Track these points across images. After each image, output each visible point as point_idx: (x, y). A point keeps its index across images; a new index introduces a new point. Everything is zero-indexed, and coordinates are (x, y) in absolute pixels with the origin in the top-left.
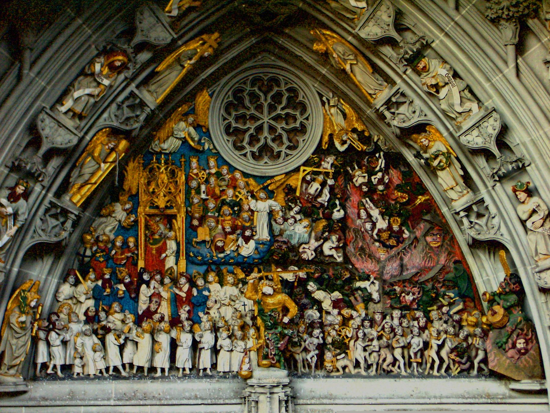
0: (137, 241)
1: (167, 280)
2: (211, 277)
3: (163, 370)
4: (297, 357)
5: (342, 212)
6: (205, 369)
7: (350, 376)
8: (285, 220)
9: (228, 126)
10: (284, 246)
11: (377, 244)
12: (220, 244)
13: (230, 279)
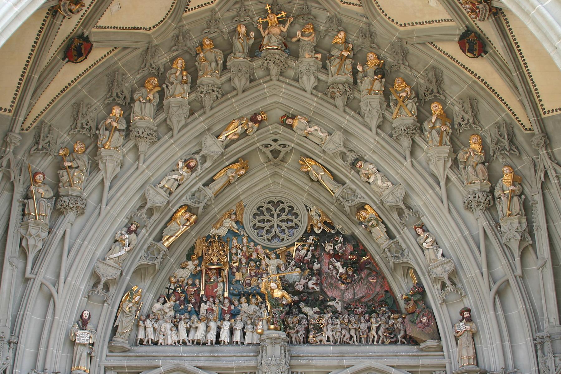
0: (200, 282)
1: (217, 301)
2: (243, 299)
3: (212, 344)
4: (292, 335)
5: (319, 265)
6: (237, 342)
7: (324, 345)
8: (286, 269)
9: (255, 225)
10: (285, 283)
11: (340, 282)
12: (248, 281)
13: (254, 301)
